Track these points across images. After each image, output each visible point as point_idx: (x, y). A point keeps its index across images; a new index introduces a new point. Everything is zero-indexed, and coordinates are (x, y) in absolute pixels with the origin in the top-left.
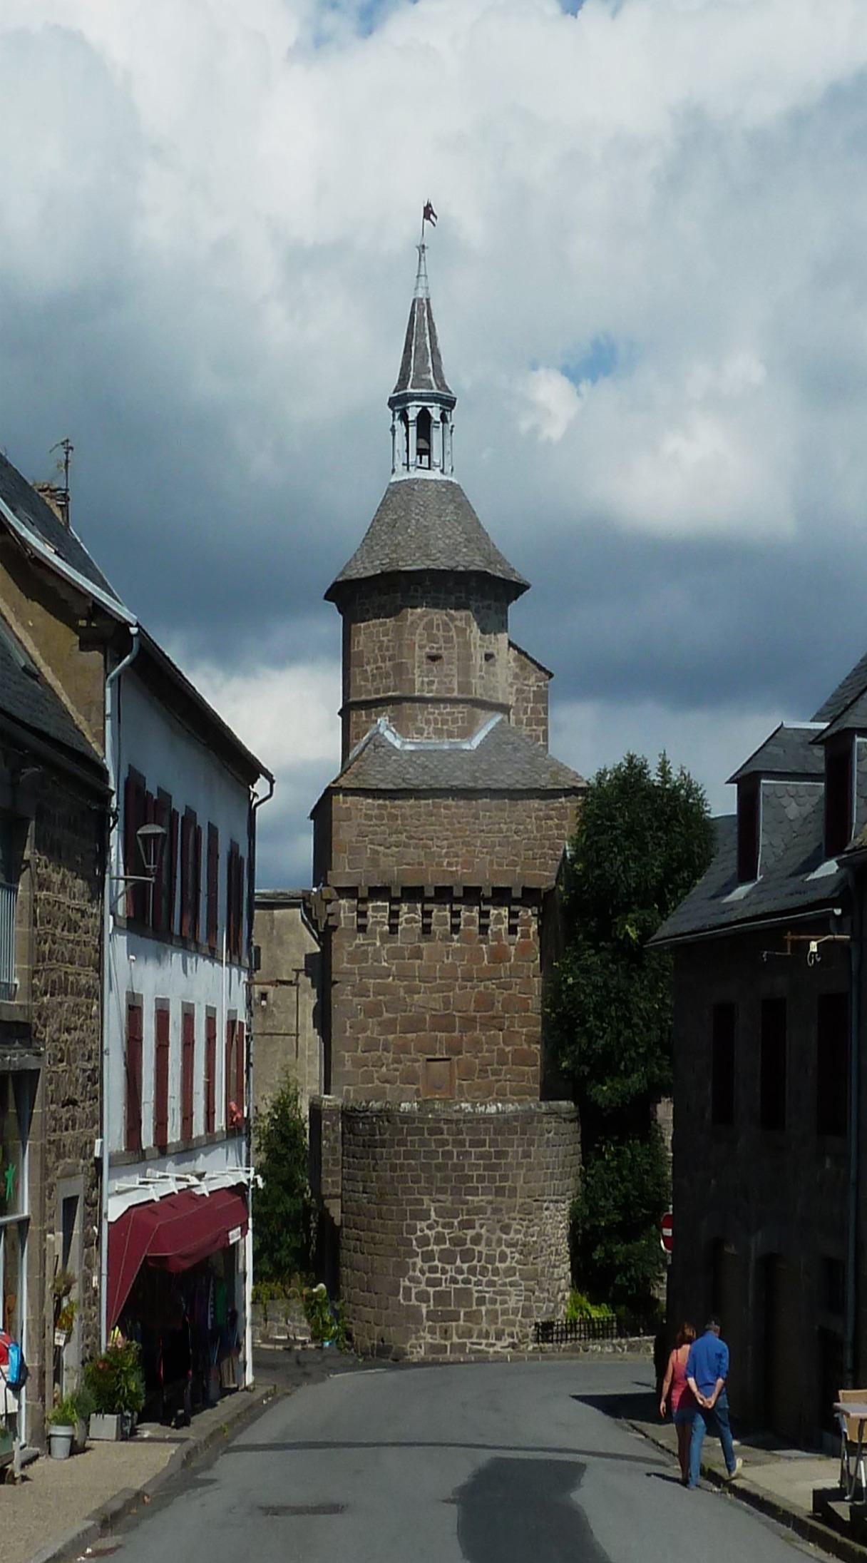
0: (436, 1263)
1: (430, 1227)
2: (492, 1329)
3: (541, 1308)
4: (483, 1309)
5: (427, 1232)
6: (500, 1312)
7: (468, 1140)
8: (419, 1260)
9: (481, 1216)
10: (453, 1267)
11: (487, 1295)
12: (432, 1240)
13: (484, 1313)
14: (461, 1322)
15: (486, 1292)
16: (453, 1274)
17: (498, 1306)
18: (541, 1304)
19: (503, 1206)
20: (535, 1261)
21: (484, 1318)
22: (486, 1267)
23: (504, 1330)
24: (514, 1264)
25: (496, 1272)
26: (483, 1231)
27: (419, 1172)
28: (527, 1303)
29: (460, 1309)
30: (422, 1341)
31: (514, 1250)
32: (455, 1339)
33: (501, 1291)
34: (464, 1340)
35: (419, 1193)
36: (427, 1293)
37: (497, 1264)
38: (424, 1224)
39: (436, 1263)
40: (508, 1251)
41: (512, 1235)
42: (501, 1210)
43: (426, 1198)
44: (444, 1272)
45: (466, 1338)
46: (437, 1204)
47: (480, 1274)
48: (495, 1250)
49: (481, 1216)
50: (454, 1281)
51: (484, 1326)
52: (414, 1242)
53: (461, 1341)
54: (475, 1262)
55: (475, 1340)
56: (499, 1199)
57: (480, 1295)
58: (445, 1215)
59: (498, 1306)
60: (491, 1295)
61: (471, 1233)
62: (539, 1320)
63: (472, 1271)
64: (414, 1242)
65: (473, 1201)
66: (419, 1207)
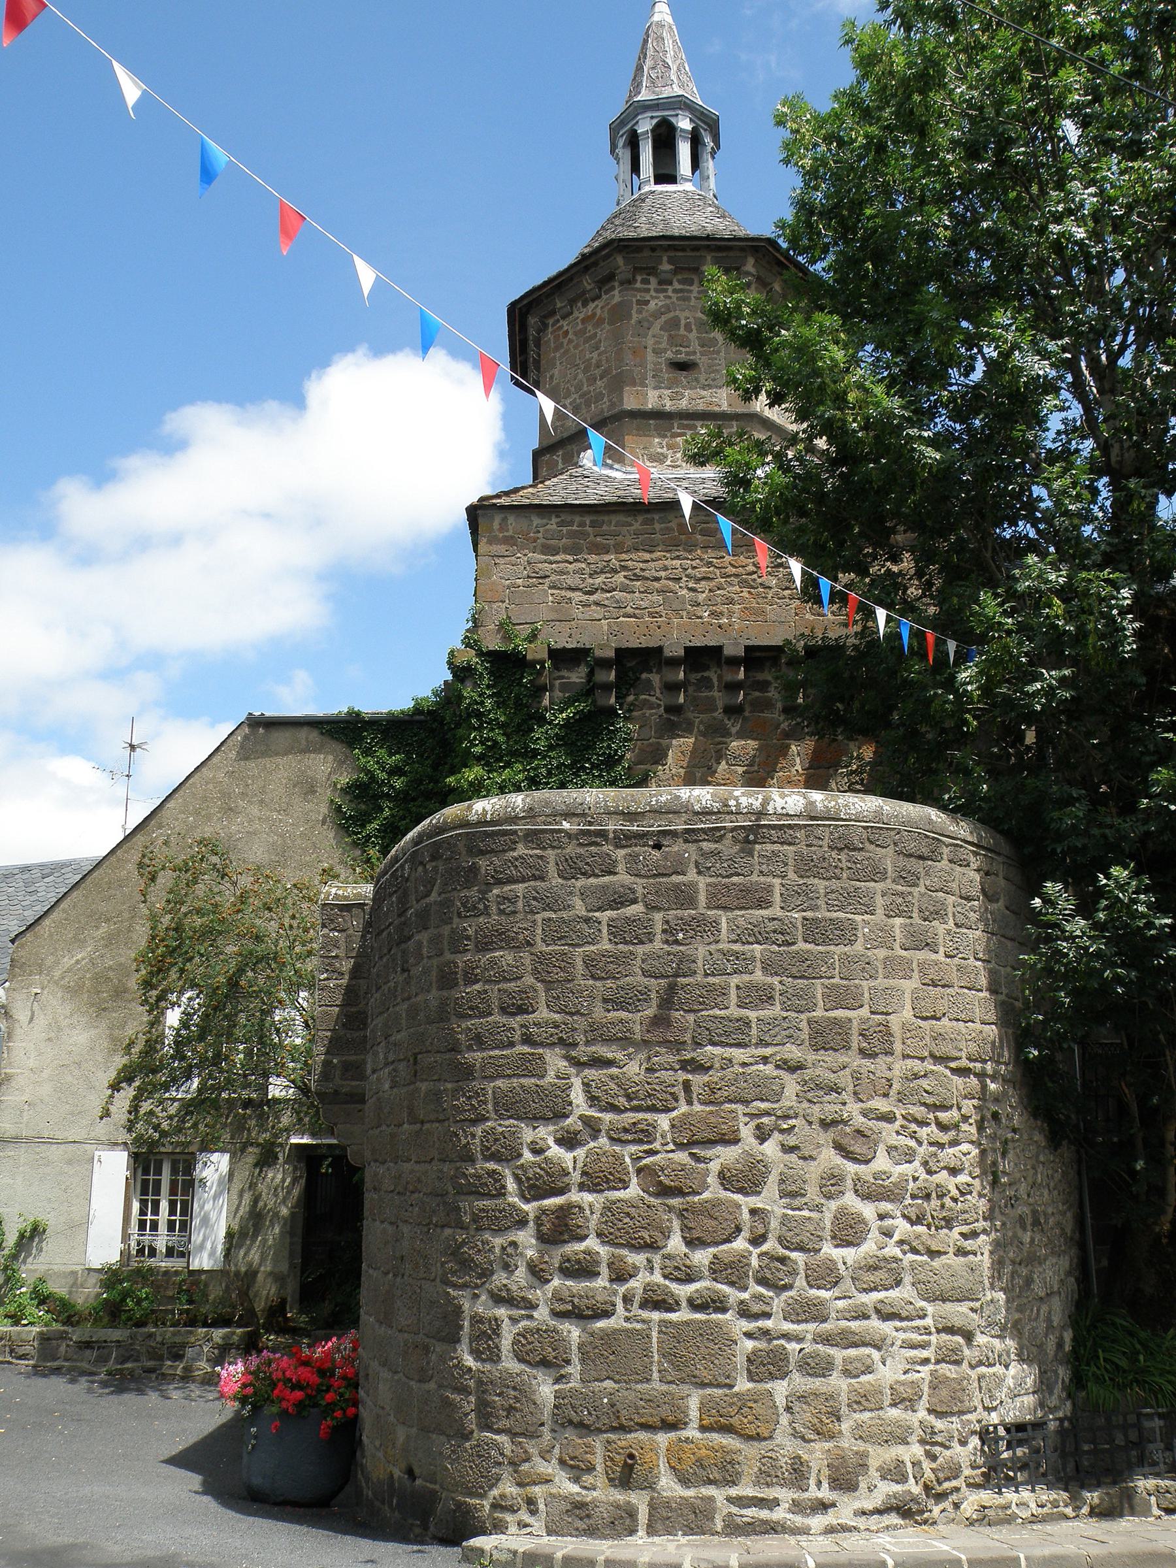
0: (592, 1243)
1: (569, 1141)
2: (817, 1455)
3: (1001, 1380)
4: (780, 1389)
7: (702, 887)
8: (526, 1238)
9: (763, 1106)
10: (657, 1259)
11: (793, 1347)
12: (576, 1177)
13: (781, 1401)
14: (692, 1432)
15: (786, 1336)
16: (657, 1278)
17: (838, 1383)
18: (998, 1369)
19: (845, 1079)
20: (969, 1244)
21: (784, 1419)
23: (864, 1455)
24: (893, 1251)
25: (826, 1276)
26: (770, 1148)
27: (529, 980)
28: (946, 1370)
29: (685, 1389)
30: (537, 1490)
31: (886, 1206)
32: (668, 1485)
33: (844, 1333)
35: (527, 1040)
36: (558, 1342)
37: (829, 1250)
38: (545, 1133)
39: (592, 1243)
40: (868, 1211)
41: (882, 1162)
42: (836, 1089)
43: (555, 1062)
45: (711, 1482)
46: (592, 1073)
47: (762, 1281)
48: (818, 1208)
49: (763, 1106)
50: (657, 1301)
51: (785, 1445)
52: (511, 1185)
53: (690, 1493)
54: (740, 1244)
55: (746, 1490)
56: (829, 1057)
58: (622, 1101)
59: (838, 1383)
61: (725, 1155)
62: (994, 1418)
63: (721, 1270)
64: (511, 1185)
66: (528, 1082)
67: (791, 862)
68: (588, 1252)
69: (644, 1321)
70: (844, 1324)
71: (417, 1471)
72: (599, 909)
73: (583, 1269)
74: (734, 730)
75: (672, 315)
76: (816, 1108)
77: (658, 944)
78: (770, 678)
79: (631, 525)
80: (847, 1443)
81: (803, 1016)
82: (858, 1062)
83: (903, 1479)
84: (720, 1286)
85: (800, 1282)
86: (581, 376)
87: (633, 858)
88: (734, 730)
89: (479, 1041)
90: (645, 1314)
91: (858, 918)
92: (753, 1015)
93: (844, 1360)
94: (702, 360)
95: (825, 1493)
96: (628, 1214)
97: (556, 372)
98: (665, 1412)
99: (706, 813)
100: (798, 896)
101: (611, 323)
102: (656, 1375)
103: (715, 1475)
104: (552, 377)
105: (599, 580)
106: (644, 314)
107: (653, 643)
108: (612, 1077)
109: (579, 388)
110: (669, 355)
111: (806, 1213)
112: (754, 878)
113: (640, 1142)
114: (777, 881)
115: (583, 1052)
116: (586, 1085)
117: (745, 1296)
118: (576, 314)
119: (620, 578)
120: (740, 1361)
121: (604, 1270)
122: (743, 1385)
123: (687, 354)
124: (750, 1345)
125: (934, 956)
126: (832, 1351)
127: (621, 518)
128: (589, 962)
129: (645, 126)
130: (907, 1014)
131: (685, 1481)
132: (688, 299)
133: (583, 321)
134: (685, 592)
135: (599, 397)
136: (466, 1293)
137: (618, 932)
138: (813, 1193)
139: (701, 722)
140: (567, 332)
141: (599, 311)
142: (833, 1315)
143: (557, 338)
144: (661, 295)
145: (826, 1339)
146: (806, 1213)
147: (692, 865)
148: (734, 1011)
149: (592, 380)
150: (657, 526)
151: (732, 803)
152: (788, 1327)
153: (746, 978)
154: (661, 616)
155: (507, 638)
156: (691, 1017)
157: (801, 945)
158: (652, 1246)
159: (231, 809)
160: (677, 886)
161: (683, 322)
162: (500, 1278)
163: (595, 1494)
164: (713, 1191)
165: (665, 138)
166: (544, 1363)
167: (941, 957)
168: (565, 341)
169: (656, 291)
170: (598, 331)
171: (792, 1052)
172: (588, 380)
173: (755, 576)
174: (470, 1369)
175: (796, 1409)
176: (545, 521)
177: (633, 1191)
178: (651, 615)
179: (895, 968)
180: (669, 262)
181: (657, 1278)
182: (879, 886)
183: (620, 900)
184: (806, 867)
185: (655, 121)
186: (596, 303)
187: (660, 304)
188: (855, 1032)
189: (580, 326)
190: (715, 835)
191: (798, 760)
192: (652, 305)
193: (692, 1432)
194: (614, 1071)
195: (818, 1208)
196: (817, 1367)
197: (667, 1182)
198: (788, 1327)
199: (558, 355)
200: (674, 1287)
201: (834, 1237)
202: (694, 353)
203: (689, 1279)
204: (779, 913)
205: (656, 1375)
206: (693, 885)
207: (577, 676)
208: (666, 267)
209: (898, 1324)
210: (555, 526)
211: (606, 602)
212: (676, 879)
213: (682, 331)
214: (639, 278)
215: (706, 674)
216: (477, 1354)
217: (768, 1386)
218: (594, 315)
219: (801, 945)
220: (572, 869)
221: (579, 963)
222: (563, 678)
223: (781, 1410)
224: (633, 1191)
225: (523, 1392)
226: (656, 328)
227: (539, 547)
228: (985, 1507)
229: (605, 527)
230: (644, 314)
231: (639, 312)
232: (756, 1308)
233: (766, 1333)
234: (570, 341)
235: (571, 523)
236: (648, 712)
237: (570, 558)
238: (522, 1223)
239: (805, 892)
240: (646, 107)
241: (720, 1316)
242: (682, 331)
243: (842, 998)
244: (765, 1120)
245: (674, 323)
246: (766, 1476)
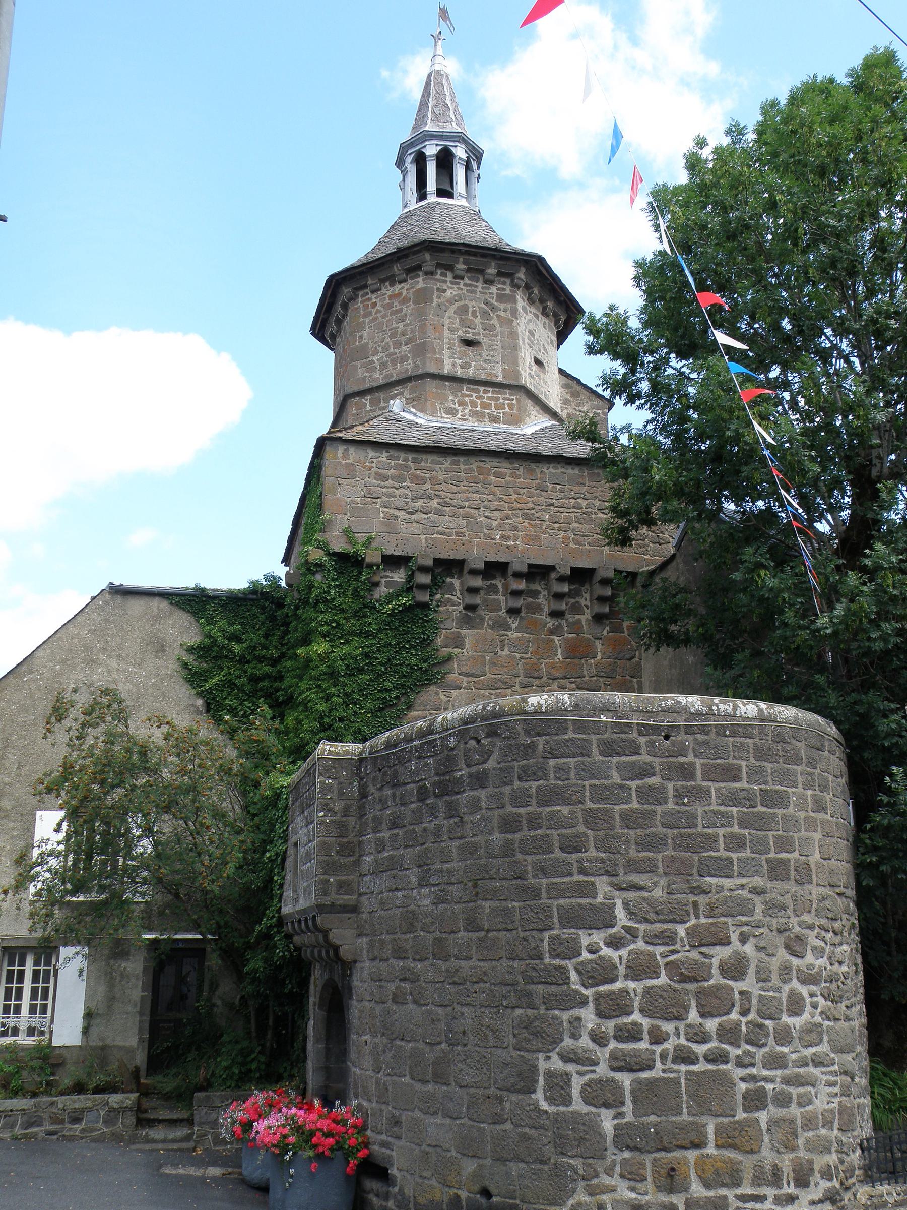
0: (636, 1017)
1: (615, 943)
2: (786, 1163)
4: (763, 1116)
5: (606, 951)
6: (799, 1122)
8: (588, 1016)
9: (744, 919)
10: (682, 1026)
11: (769, 1087)
12: (622, 970)
13: (764, 1126)
14: (711, 1150)
15: (766, 1079)
16: (683, 1041)
17: (794, 1111)
19: (788, 900)
21: (766, 1139)
22: (761, 1026)
23: (811, 1162)
24: (818, 1019)
25: (784, 1036)
27: (581, 829)
29: (704, 1119)
31: (813, 988)
33: (798, 1076)
34: (723, 1192)
35: (582, 871)
36: (616, 1087)
37: (786, 1019)
38: (598, 937)
39: (636, 1017)
40: (804, 990)
41: (810, 958)
42: (784, 908)
43: (603, 886)
44: (658, 1038)
45: (723, 1185)
46: (631, 895)
47: (749, 1042)
48: (778, 990)
49: (744, 919)
50: (684, 1057)
51: (767, 1155)
52: (574, 976)
53: (711, 1194)
54: (734, 1016)
55: (747, 1190)
56: (778, 885)
57: (751, 1086)
58: (652, 916)
59: (794, 1111)
60: (778, 1086)
61: (720, 953)
63: (729, 1034)
64: (574, 976)
65: (721, 888)
66: (587, 901)
67: (751, 751)
68: (635, 1024)
69: (675, 1072)
70: (796, 1070)
71: (493, 1190)
72: (632, 779)
73: (633, 1033)
74: (514, 626)
75: (463, 302)
76: (774, 921)
77: (671, 805)
78: (539, 589)
79: (443, 464)
80: (802, 1153)
81: (763, 857)
82: (794, 888)
83: (830, 1180)
84: (724, 1046)
85: (771, 1041)
86: (387, 340)
87: (651, 744)
88: (514, 626)
89: (543, 871)
90: (676, 1067)
91: (790, 790)
92: (734, 856)
93: (799, 1096)
94: (485, 341)
95: (791, 1190)
96: (661, 996)
97: (365, 334)
98: (693, 1136)
99: (699, 714)
100: (756, 774)
101: (415, 303)
102: (685, 1110)
103: (727, 1180)
104: (361, 337)
105: (419, 504)
106: (442, 300)
107: (459, 557)
108: (644, 899)
109: (385, 349)
110: (460, 333)
111: (771, 993)
112: (731, 761)
113: (667, 944)
114: (744, 764)
115: (624, 878)
116: (626, 905)
117: (739, 1052)
118: (384, 291)
119: (434, 503)
120: (739, 1098)
121: (646, 1035)
122: (741, 1115)
123: (474, 334)
124: (743, 1086)
125: (826, 817)
126: (791, 1089)
127: (435, 458)
128: (625, 816)
129: (431, 150)
130: (817, 855)
131: (707, 1186)
132: (474, 292)
133: (390, 297)
134: (482, 519)
135: (404, 359)
136: (541, 1056)
137: (645, 794)
138: (775, 980)
139: (490, 618)
140: (375, 304)
141: (404, 293)
142: (790, 1064)
143: (366, 307)
144: (455, 287)
145: (787, 1081)
146: (771, 993)
147: (691, 751)
148: (722, 853)
149: (398, 345)
150: (462, 467)
151: (715, 708)
152: (766, 1073)
153: (729, 830)
154: (464, 536)
155: (352, 541)
156: (696, 857)
157: (760, 808)
158: (678, 1018)
159: (93, 661)
160: (682, 765)
161: (471, 309)
162: (568, 1042)
163: (647, 1198)
164: (716, 979)
165: (445, 160)
166: (606, 1105)
167: (828, 817)
168: (374, 311)
169: (452, 283)
170: (404, 307)
171: (758, 881)
172: (394, 343)
173: (533, 511)
174: (546, 1112)
175: (773, 1131)
176: (378, 454)
177: (663, 979)
178: (457, 534)
179: (811, 824)
180: (464, 263)
181: (683, 1041)
182: (799, 769)
183: (646, 771)
184: (762, 754)
185: (439, 148)
186: (403, 285)
187: (454, 293)
188: (792, 868)
189: (387, 301)
190: (704, 730)
191: (559, 651)
192: (448, 293)
193: (711, 1150)
194: (645, 894)
195: (778, 990)
196: (783, 1100)
197: (686, 973)
198: (766, 1073)
199: (367, 320)
200: (695, 1047)
201: (788, 1010)
202: (479, 334)
203: (704, 1041)
204: (746, 786)
205: (685, 1110)
206: (692, 765)
207: (399, 576)
208: (461, 266)
209: (824, 1069)
210: (385, 459)
211: (424, 522)
212: (682, 759)
213: (470, 316)
214: (439, 271)
215: (494, 582)
216: (550, 1100)
217: (756, 1115)
218: (400, 294)
219: (760, 808)
220: (609, 749)
221: (617, 817)
222: (387, 577)
223: (764, 1132)
224: (663, 979)
225: (592, 1127)
226: (451, 311)
227: (373, 474)
228: (872, 1196)
229: (423, 464)
230: (442, 300)
231: (439, 297)
232: (747, 1060)
233: (753, 1078)
235: (397, 458)
236: (451, 608)
237: (397, 485)
238: (584, 1003)
239: (760, 771)
240: (432, 136)
241: (724, 1067)
242: (470, 316)
243: (784, 844)
244: (745, 928)
245: (463, 310)
246: (758, 1181)
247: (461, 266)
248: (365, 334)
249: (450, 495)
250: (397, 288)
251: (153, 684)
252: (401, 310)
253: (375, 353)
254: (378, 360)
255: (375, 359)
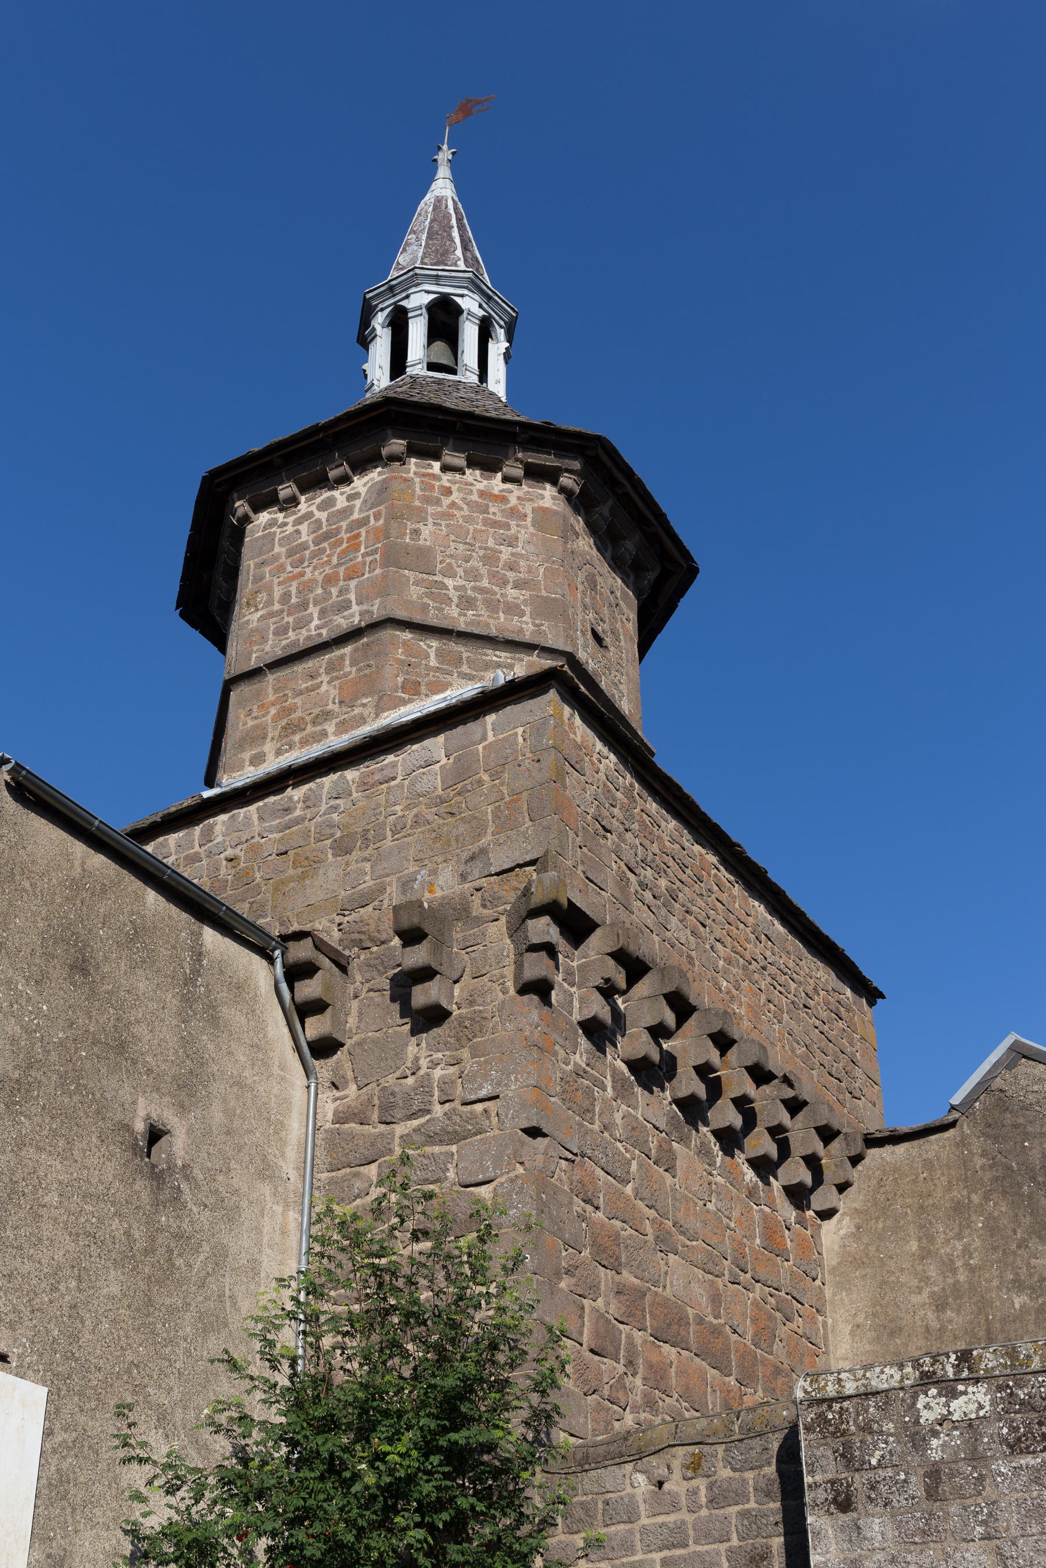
140: (448, 492)
141: (513, 501)
168: (446, 501)
170: (513, 523)
186: (508, 486)
189: (475, 497)
199: (430, 509)
208: (605, 510)
218: (502, 499)
234: (453, 504)
247: (605, 510)
248: (426, 531)
249: (678, 883)
250: (496, 483)
251: (61, 1043)
252: (508, 527)
253: (449, 573)
254: (456, 588)
255: (450, 582)
